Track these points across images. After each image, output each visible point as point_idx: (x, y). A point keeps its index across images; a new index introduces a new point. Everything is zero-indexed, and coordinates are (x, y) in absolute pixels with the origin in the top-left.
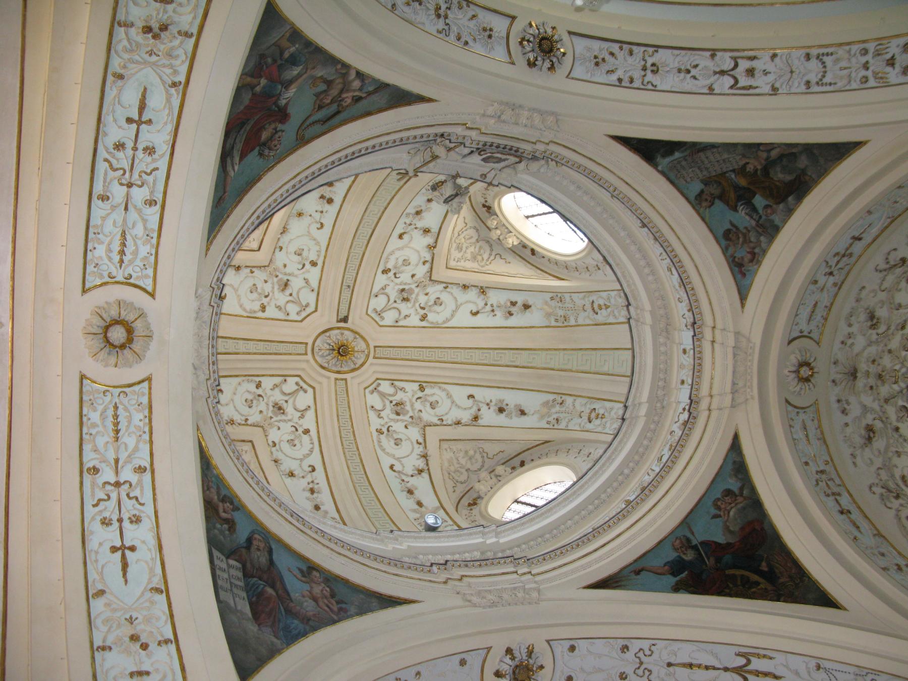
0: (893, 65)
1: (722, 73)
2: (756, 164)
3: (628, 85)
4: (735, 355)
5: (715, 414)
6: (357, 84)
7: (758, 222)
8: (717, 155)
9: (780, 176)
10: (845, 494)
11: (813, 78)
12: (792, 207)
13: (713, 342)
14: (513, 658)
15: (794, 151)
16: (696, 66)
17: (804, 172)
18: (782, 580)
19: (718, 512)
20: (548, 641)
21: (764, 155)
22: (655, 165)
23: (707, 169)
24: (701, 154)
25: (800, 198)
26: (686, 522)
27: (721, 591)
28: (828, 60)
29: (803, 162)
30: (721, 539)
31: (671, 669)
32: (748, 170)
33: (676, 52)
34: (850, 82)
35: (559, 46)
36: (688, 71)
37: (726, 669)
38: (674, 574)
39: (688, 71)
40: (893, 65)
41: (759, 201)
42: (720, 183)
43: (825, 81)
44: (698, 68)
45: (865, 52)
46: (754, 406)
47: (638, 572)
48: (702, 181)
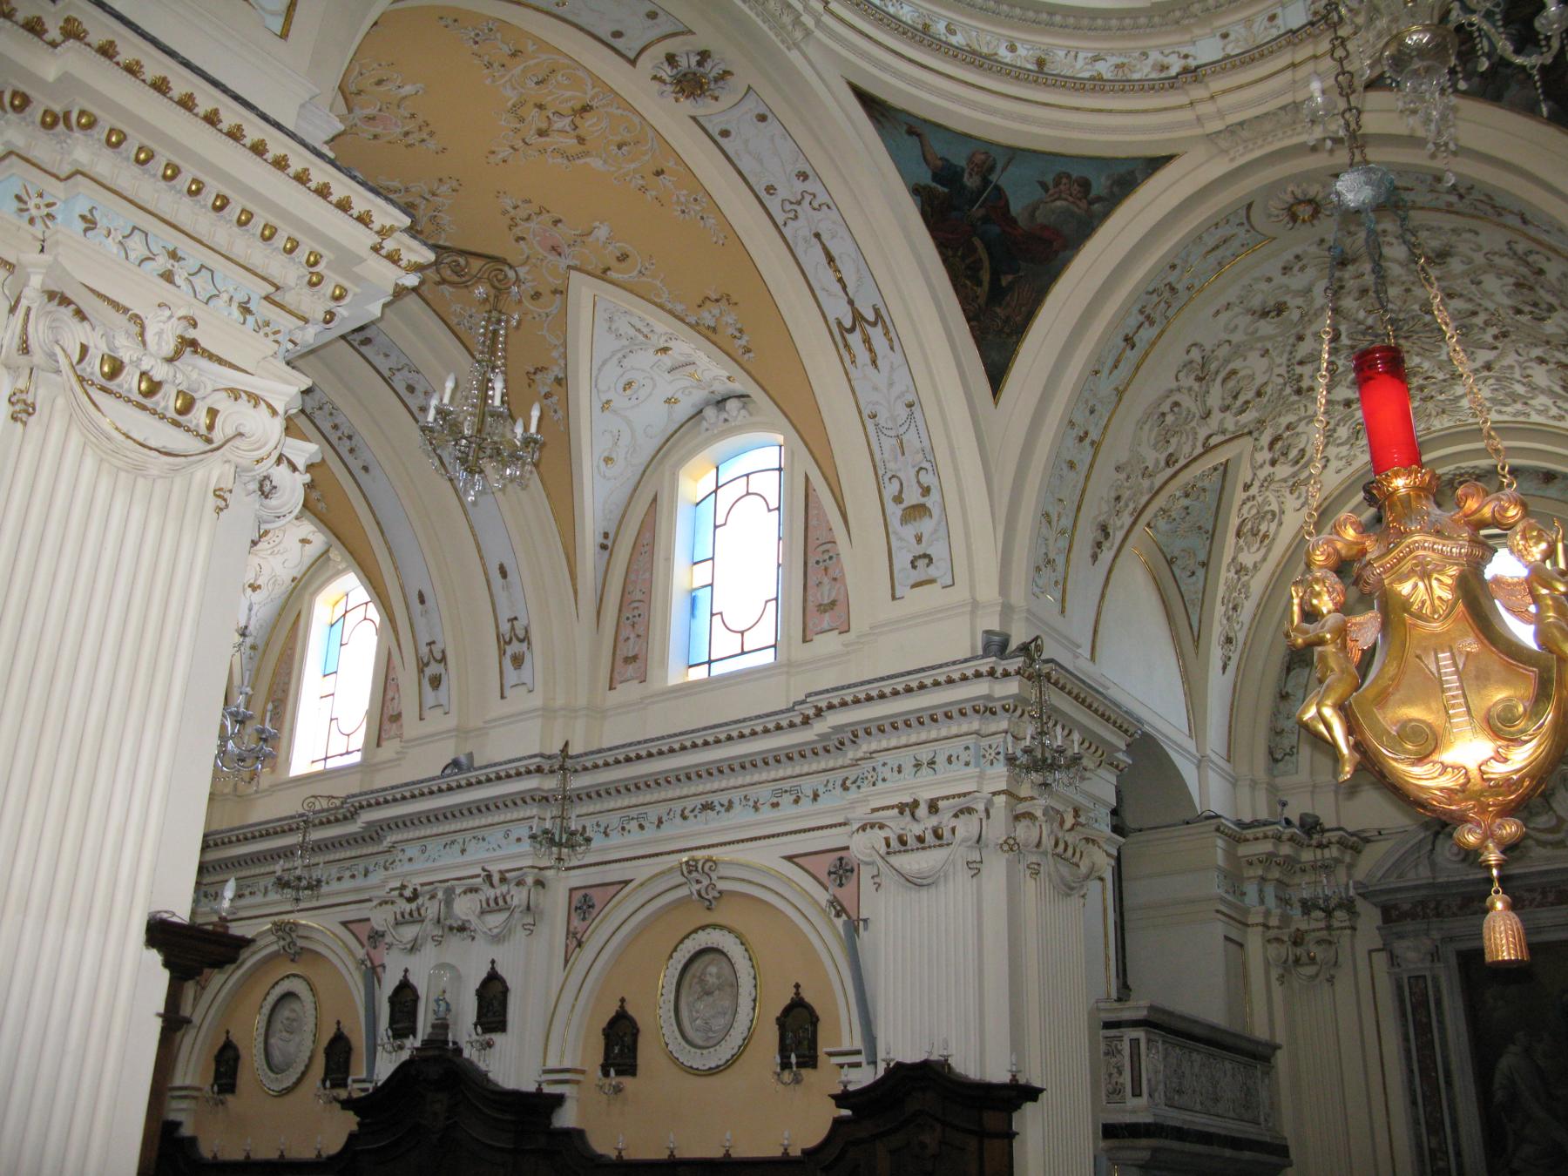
4: (1283, 108)
5: (1187, 115)
10: (1155, 331)
13: (1293, 66)
14: (700, 64)
18: (998, 310)
19: (1051, 185)
20: (749, 88)
26: (1014, 154)
27: (942, 245)
30: (1016, 207)
31: (815, 240)
37: (851, 302)
38: (936, 177)
46: (1220, 167)
47: (911, 132)
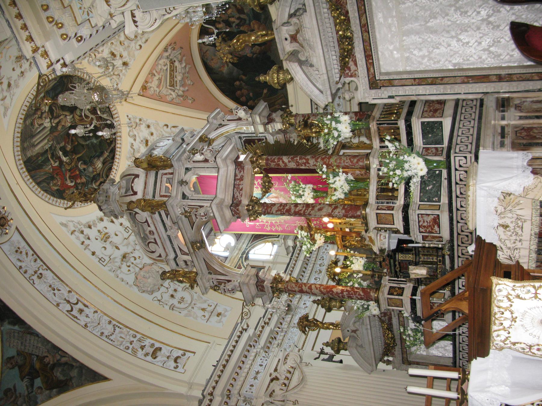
0: (143, 349)
1: (68, 302)
2: (51, 360)
3: (23, 273)
7: (29, 394)
8: (36, 342)
9: (58, 374)
11: (106, 333)
12: (52, 396)
15: (74, 364)
16: (59, 290)
17: (71, 379)
21: (59, 357)
23: (25, 346)
24: (29, 335)
25: (59, 393)
28: (117, 330)
29: (74, 373)
32: (45, 360)
33: (55, 277)
34: (121, 345)
35: (8, 228)
36: (54, 290)
39: (54, 290)
40: (143, 349)
41: (38, 382)
42: (26, 359)
43: (110, 337)
44: (59, 292)
45: (135, 337)
48: (18, 351)
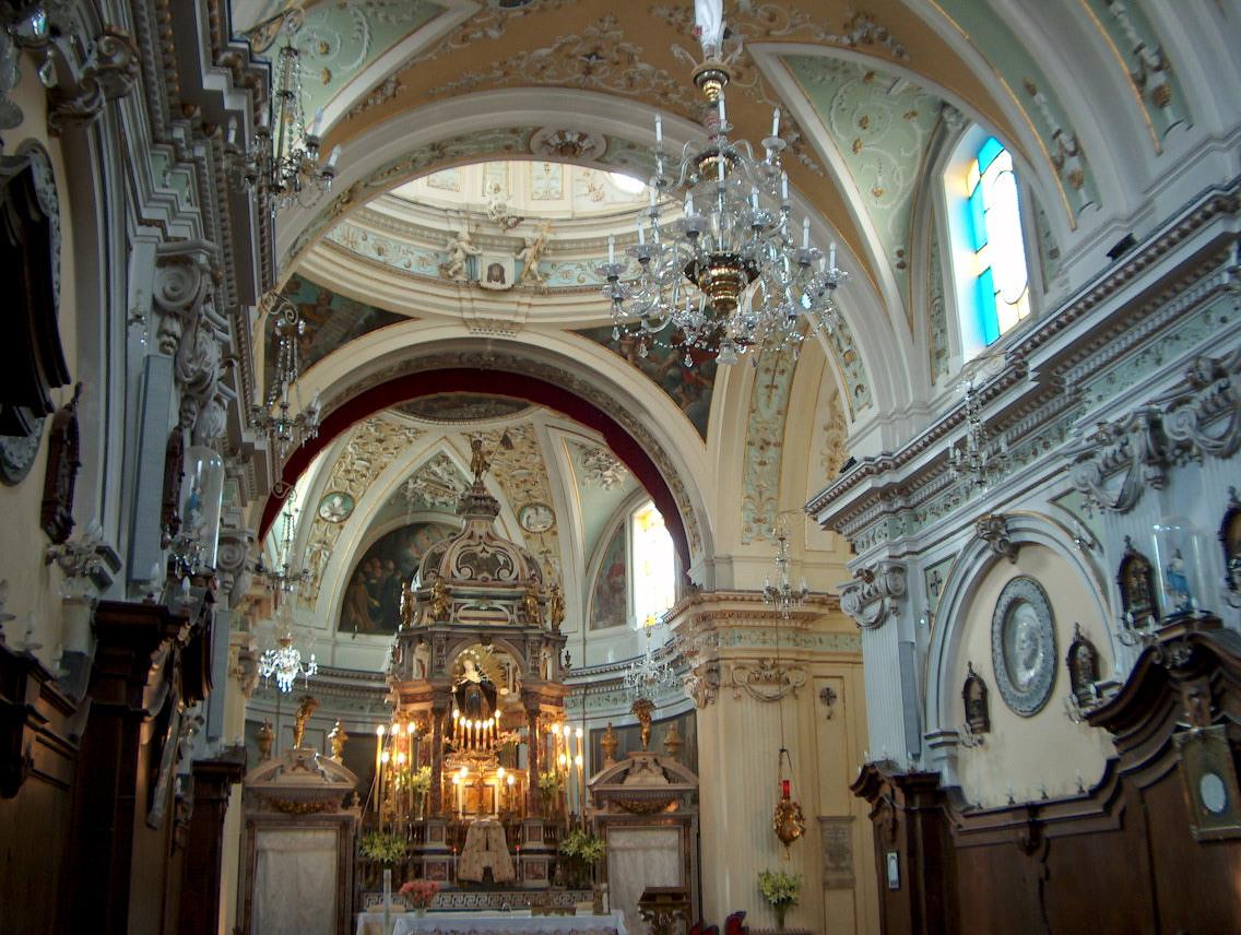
6: (625, 350)
22: (373, 308)
24: (344, 331)
25: (266, 345)
